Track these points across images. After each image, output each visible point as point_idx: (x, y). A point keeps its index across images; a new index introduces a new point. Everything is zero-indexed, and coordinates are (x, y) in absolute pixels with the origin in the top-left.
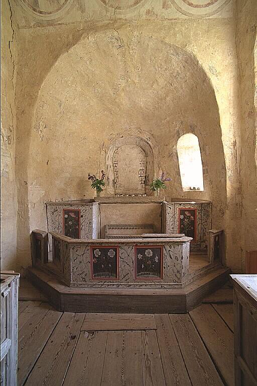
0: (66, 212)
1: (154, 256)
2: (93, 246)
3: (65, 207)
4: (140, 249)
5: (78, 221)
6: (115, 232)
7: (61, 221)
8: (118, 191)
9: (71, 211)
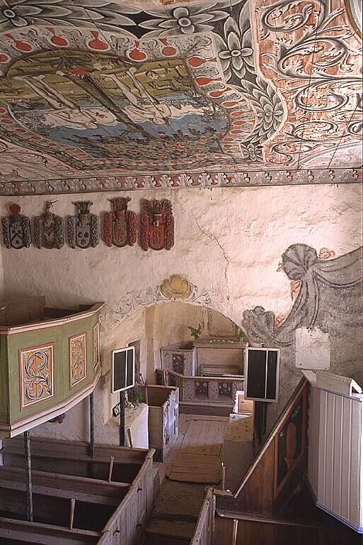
0: (174, 355)
1: (228, 387)
2: (195, 380)
3: (174, 353)
4: (221, 383)
5: (183, 362)
6: (208, 369)
7: (171, 361)
8: (213, 333)
9: (178, 355)
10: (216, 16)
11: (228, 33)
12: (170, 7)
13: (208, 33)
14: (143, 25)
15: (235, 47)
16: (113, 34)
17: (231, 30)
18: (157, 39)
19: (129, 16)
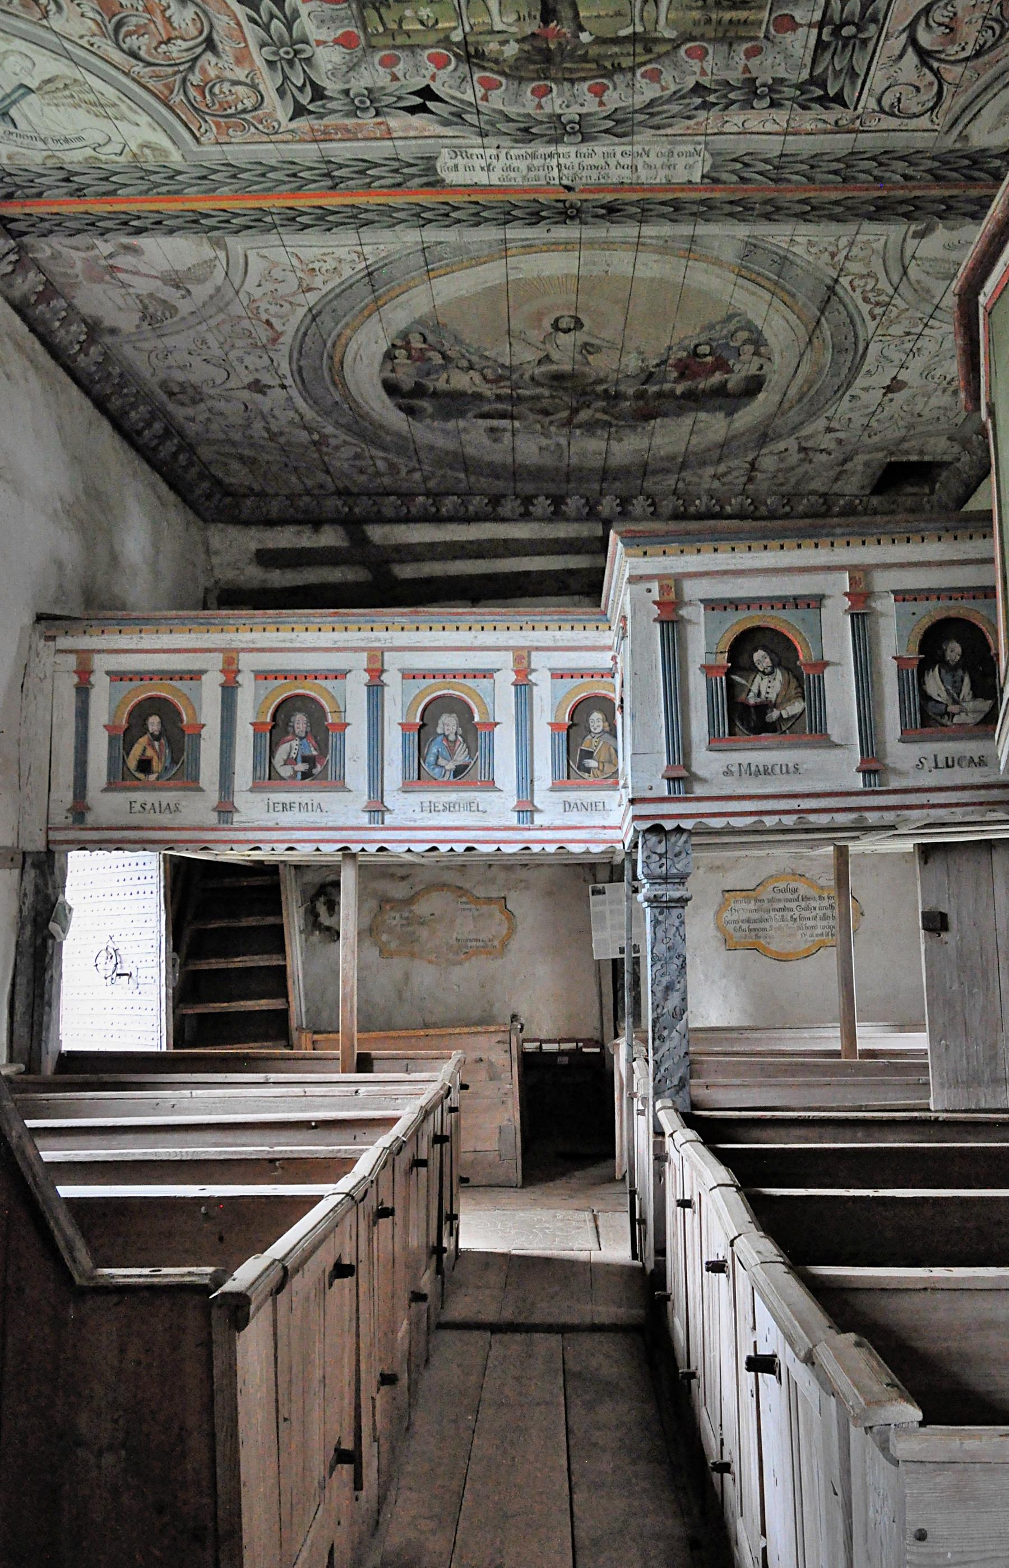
10: (323, 106)
11: (304, 85)
12: (379, 120)
13: (332, 87)
14: (419, 100)
15: (291, 63)
16: (459, 95)
17: (301, 89)
18: (403, 81)
19: (432, 113)
